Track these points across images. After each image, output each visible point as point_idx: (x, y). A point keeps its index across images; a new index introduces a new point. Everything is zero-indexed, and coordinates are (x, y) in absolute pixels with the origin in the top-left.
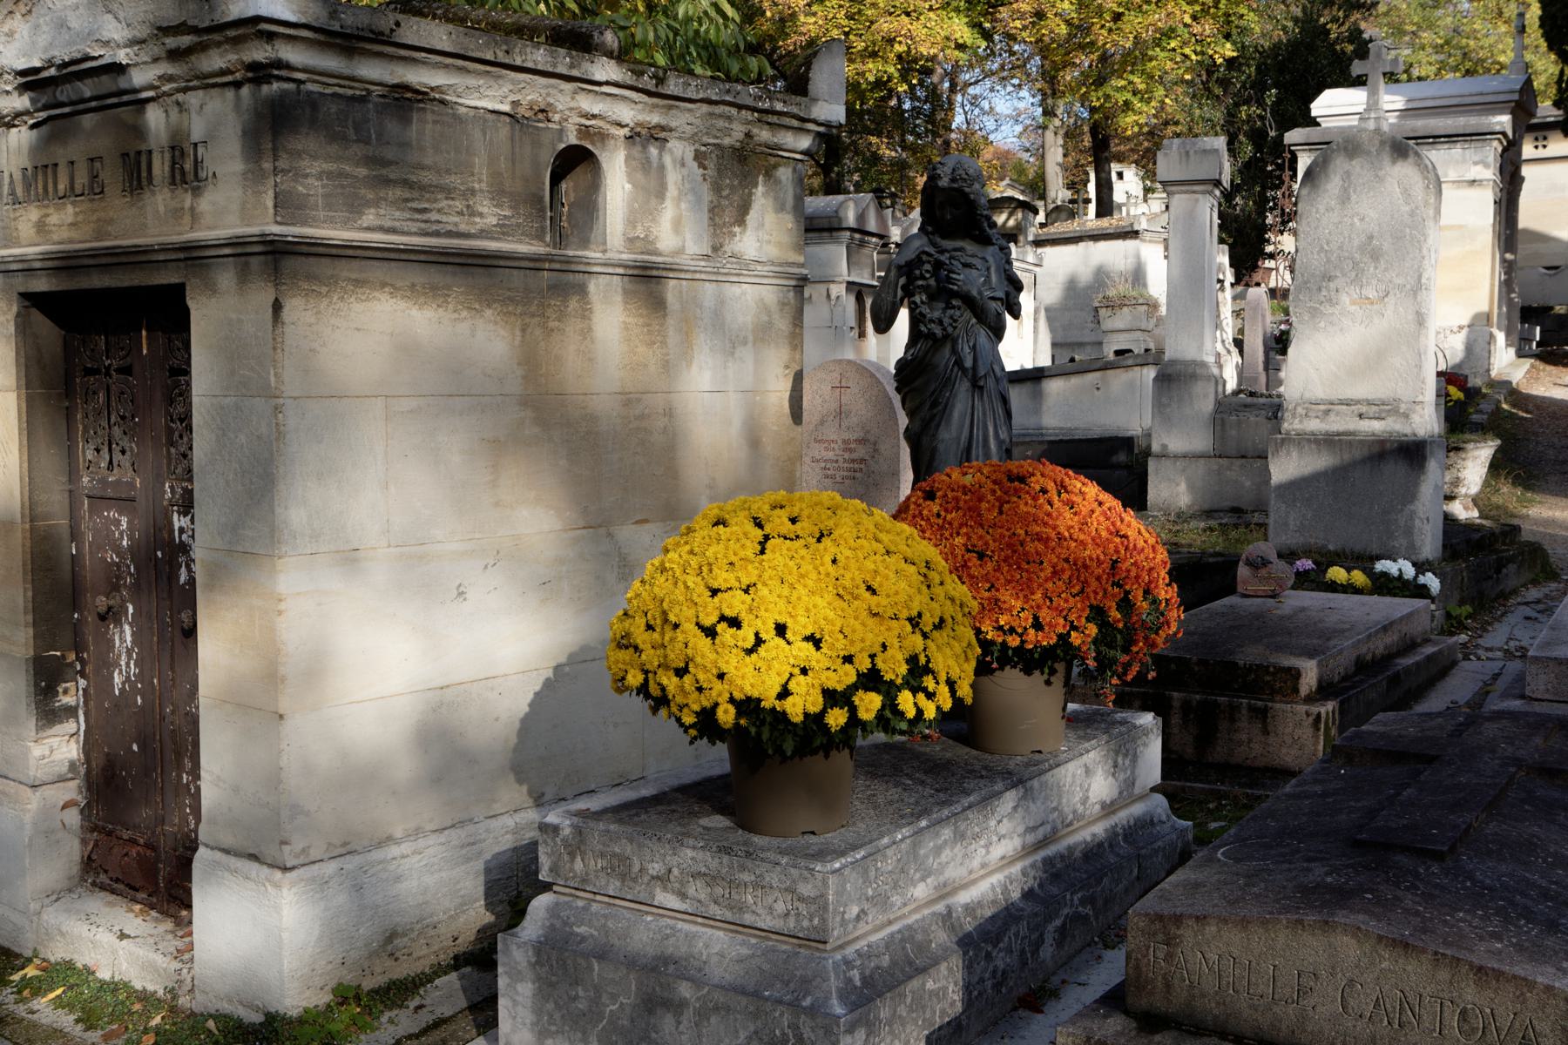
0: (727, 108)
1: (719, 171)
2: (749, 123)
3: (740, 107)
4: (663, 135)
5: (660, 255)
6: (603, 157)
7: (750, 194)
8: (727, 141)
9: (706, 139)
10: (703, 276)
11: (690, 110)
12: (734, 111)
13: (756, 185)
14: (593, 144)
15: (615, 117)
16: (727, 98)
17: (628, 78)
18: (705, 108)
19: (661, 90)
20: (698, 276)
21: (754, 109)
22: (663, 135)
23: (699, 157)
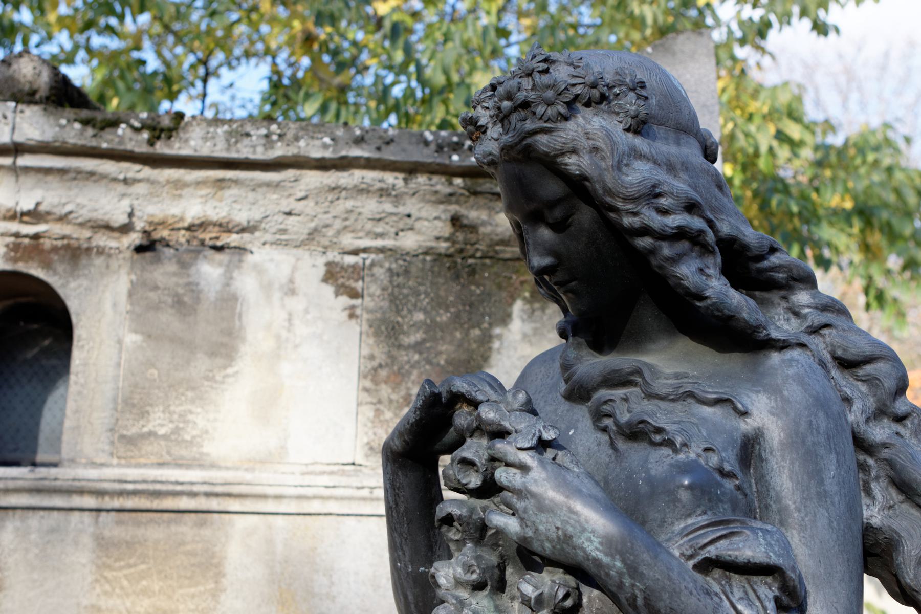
0: (371, 176)
1: (393, 299)
2: (450, 198)
3: (411, 169)
4: (233, 239)
5: (213, 466)
6: (73, 292)
7: (486, 339)
8: (410, 242)
9: (348, 241)
10: (333, 507)
11: (277, 185)
12: (391, 179)
13: (505, 319)
14: (47, 265)
15: (84, 214)
16: (356, 152)
17: (73, 132)
18: (313, 179)
19: (161, 148)
20: (315, 506)
21: (449, 172)
22: (233, 239)
23: (332, 274)
